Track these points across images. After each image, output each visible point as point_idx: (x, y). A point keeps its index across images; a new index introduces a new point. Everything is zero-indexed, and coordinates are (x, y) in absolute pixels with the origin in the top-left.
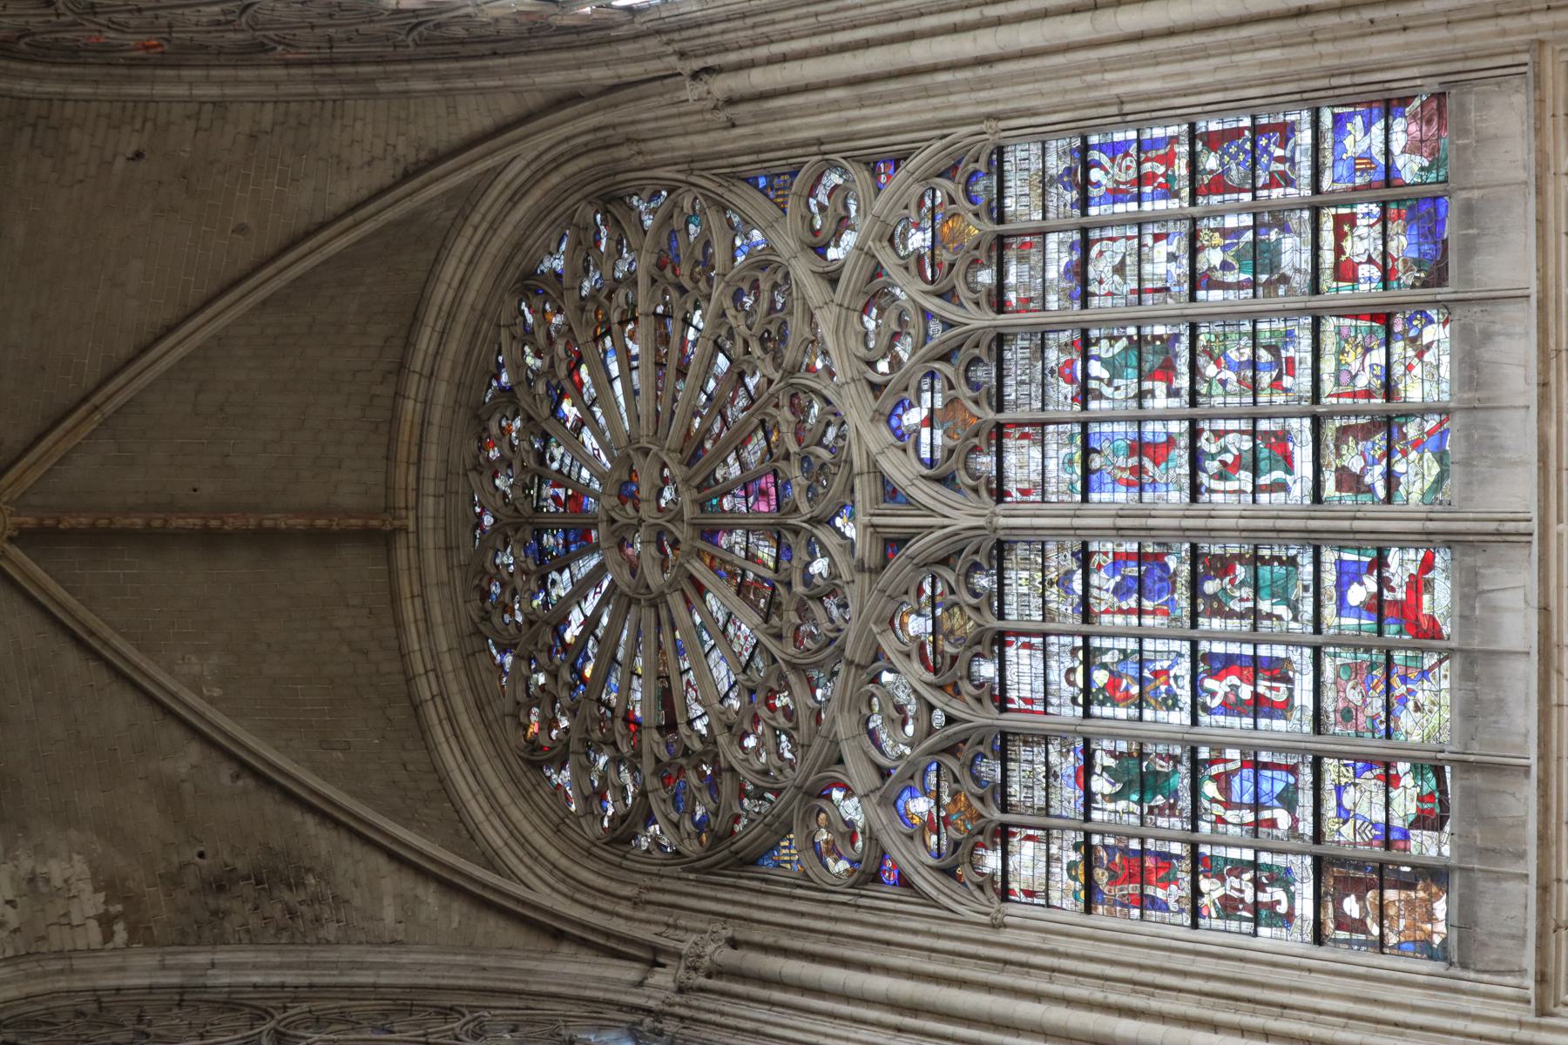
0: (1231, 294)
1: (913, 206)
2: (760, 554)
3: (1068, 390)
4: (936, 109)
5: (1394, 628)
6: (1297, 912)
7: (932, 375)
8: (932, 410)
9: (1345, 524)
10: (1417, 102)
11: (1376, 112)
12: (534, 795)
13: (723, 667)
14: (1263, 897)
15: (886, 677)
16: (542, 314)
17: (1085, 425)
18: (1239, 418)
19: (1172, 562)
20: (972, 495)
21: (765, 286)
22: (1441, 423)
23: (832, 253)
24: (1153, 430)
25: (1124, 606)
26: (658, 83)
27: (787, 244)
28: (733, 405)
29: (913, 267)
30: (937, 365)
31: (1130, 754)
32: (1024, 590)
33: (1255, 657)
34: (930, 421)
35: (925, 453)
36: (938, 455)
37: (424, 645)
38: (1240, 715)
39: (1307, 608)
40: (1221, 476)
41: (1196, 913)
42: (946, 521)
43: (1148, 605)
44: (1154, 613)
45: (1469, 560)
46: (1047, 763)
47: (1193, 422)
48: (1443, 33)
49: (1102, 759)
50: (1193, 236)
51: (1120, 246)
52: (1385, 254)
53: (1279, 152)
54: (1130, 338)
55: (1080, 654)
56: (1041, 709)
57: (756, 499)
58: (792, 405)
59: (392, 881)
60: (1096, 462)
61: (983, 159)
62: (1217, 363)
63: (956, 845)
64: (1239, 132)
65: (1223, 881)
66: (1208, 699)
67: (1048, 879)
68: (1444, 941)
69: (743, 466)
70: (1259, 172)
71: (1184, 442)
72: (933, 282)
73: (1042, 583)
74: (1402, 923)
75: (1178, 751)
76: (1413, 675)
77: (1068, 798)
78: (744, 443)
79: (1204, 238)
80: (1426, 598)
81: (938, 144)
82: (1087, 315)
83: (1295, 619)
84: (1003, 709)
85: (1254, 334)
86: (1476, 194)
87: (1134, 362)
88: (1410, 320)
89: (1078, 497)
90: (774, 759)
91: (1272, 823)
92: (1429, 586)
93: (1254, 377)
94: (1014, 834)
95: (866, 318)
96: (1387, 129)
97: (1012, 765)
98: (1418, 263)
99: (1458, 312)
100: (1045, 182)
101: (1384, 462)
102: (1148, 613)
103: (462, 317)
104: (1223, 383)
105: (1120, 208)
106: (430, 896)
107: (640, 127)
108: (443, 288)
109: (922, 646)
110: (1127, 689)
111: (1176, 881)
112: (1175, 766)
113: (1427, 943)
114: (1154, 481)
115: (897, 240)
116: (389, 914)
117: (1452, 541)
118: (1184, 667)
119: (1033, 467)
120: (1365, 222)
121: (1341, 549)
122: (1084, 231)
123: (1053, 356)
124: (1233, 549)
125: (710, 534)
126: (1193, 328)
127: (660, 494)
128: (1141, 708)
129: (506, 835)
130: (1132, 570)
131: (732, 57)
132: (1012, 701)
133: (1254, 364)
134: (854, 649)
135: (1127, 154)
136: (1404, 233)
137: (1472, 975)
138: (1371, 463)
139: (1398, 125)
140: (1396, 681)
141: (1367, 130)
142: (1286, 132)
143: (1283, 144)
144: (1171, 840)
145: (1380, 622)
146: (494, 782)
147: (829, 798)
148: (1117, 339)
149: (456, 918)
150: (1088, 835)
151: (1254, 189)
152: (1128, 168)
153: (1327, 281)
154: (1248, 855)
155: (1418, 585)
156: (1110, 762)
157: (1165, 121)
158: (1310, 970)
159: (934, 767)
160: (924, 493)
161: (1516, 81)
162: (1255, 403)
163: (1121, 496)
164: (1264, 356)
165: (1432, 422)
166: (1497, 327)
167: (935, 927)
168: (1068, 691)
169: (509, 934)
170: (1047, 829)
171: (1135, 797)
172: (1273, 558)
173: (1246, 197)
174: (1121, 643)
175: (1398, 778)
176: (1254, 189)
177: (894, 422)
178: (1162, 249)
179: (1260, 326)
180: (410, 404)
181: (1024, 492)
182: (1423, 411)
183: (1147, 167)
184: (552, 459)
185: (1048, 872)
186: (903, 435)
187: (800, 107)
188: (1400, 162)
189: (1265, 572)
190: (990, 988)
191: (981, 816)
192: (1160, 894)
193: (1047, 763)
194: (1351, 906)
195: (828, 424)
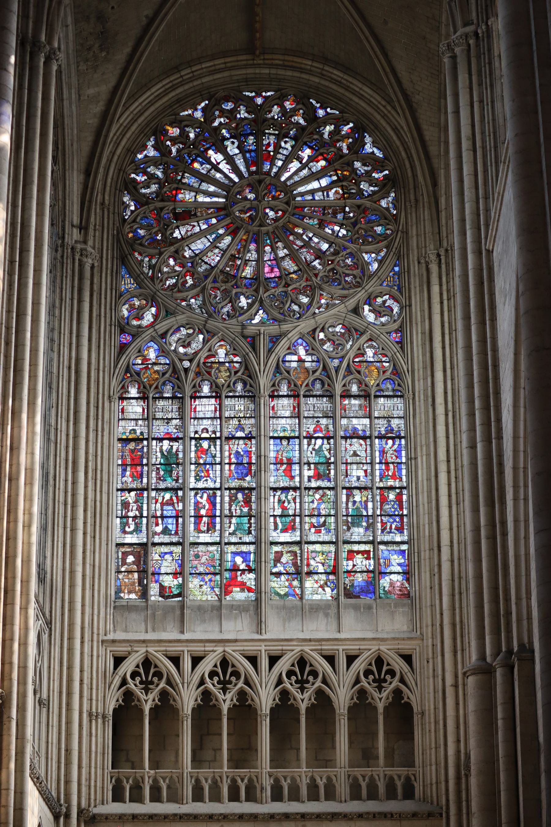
0: (344, 505)
1: (383, 352)
2: (248, 268)
3: (311, 430)
4: (419, 370)
5: (228, 576)
6: (126, 536)
7: (318, 361)
8: (304, 361)
9: (263, 559)
10: (407, 585)
11: (405, 568)
12: (143, 135)
13: (201, 246)
14: (131, 519)
15: (201, 337)
16: (347, 136)
17: (298, 437)
18: (300, 509)
19: (248, 478)
20: (272, 383)
21: (355, 272)
22: (298, 595)
23: (366, 308)
24: (296, 467)
25: (232, 456)
26: (437, 231)
27: (371, 286)
28: (308, 252)
29: (359, 352)
30: (322, 362)
31: (177, 459)
32: (237, 409)
33: (215, 516)
34: (300, 360)
35: (288, 358)
36: (287, 364)
37: (204, 70)
38: (195, 509)
39: (233, 539)
40: (279, 500)
41: (122, 490)
42: (262, 373)
43: (233, 467)
44: (230, 470)
45: (252, 608)
46: (172, 419)
47: (299, 488)
48: (429, 604)
49: (175, 445)
50: (365, 488)
51: (363, 454)
52: (356, 572)
53: (393, 527)
54: (330, 459)
55: (213, 436)
56: (192, 416)
57: (269, 266)
58: (307, 286)
59: (105, 89)
60: (285, 442)
61: (399, 388)
62: (320, 499)
63: (138, 374)
64: (401, 508)
65: (135, 502)
66: (199, 495)
67: (129, 419)
68: (122, 598)
69: (283, 258)
70: (387, 518)
71: (292, 484)
72: (353, 362)
73: (239, 417)
74: (127, 580)
75: (180, 481)
76: (212, 584)
77: (160, 429)
78: (292, 259)
79: (365, 493)
80: (238, 589)
81: (406, 369)
82: (338, 438)
83: (230, 534)
84: (191, 397)
85: (330, 515)
86: (375, 611)
87: (321, 461)
88: (333, 582)
89: (271, 435)
90: (166, 276)
91: (157, 525)
92: (242, 590)
93: (314, 515)
94: (144, 403)
95: (341, 326)
96: (399, 573)
97: (170, 401)
98: (352, 586)
99: (335, 603)
100: (389, 418)
101: (285, 572)
102: (230, 467)
103: (347, 94)
104: (313, 502)
105: (377, 454)
106: (98, 108)
107: (422, 209)
108: (360, 85)
109: (214, 356)
110: (201, 457)
111: (133, 481)
112: (174, 480)
113: (121, 592)
114: (278, 470)
115: (370, 343)
116: (91, 91)
117: (258, 601)
118: (211, 485)
119: (283, 412)
120: (367, 564)
121: (255, 553)
122: (370, 437)
123: (324, 421)
124: (254, 506)
125: (257, 239)
126: (332, 489)
127: (272, 209)
128: (195, 464)
129: (125, 124)
130: (245, 460)
131: (444, 279)
132: (194, 402)
133: (319, 515)
134: (211, 324)
135: (397, 457)
136: (363, 580)
137: (112, 612)
138: (284, 564)
139: (400, 577)
140: (210, 576)
141: (399, 565)
142: (400, 530)
143: (397, 529)
144: (148, 478)
145: (229, 570)
146: (146, 114)
147: (152, 306)
148: (330, 453)
149: (91, 122)
150: (147, 439)
151: (381, 515)
152: (392, 458)
153: (347, 547)
154: (145, 514)
155: (243, 586)
156: (174, 450)
157: (407, 476)
158: (107, 544)
159: (168, 362)
161: (411, 627)
162: (306, 516)
163: (272, 454)
164: (322, 520)
165: (298, 591)
166: (330, 619)
167: (107, 369)
168: (199, 429)
169: (86, 148)
170: (148, 419)
171: (162, 461)
172: (250, 524)
173: (378, 512)
174: (218, 455)
175: (176, 578)
176: (381, 515)
177: (300, 341)
178: (361, 473)
179: (333, 517)
180: (310, 63)
181: (273, 408)
182: (302, 587)
183: (391, 466)
184: (286, 142)
185: (132, 419)
186: (295, 346)
187: (423, 296)
188: (387, 578)
189: (246, 520)
190: (88, 403)
191: (150, 387)
192: (128, 473)
193: (172, 419)
194: (130, 559)
195: (300, 307)
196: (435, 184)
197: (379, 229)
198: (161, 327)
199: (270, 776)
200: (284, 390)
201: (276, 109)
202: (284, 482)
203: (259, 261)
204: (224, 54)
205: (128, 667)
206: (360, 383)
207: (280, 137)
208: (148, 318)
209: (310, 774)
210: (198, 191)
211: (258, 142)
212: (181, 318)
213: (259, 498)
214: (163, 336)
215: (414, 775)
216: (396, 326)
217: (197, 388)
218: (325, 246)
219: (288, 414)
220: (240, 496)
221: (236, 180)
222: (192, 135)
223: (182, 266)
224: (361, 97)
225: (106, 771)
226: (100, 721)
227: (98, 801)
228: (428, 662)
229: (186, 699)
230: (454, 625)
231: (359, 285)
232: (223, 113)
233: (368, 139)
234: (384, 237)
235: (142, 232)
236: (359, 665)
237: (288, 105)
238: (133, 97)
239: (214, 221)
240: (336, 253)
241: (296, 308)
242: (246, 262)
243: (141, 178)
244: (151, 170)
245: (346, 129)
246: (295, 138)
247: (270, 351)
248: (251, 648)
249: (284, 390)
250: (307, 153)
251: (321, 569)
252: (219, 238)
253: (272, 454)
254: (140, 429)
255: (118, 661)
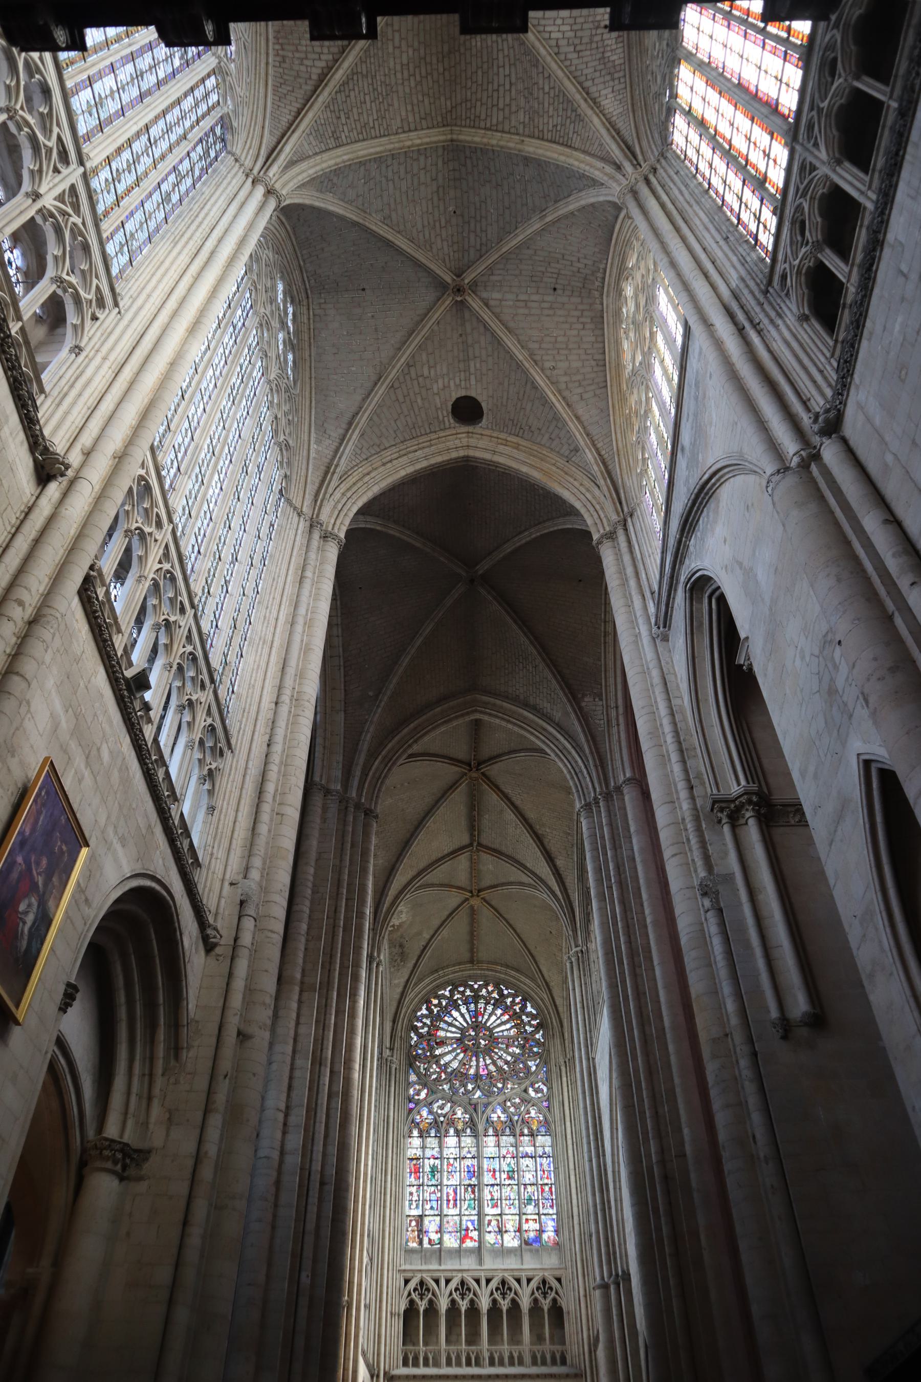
15: (449, 1105)
16: (518, 1003)
19: (473, 1179)
24: (497, 1174)
27: (532, 1078)
34: (499, 1117)
39: (466, 1213)
77: (428, 1153)
106: (400, 990)
116: (396, 982)
123: (511, 1149)
142: (552, 1207)
153: (524, 1217)
160: (485, 1116)
194: (414, 1223)
196: (562, 1026)
197: (535, 1050)
198: (430, 1100)
200: (491, 1132)
201: (484, 990)
202: (492, 1182)
203: (478, 1066)
204: (460, 964)
205: (412, 1285)
206: (529, 1128)
207: (487, 1003)
208: (423, 1095)
210: (447, 1031)
211: (476, 1006)
212: (439, 1095)
213: (479, 1190)
214: (431, 1104)
216: (545, 1098)
217: (447, 1131)
218: (509, 1058)
219: (493, 1144)
220: (469, 1189)
221: (465, 1025)
222: (444, 1003)
223: (440, 1068)
224: (525, 984)
230: (582, 1261)
231: (527, 1077)
232: (459, 992)
233: (529, 1005)
234: (538, 1053)
235: (420, 1052)
236: (534, 1284)
237: (490, 988)
238: (416, 985)
239: (455, 1046)
240: (515, 1062)
241: (495, 1089)
242: (471, 1067)
243: (419, 1024)
244: (424, 1020)
245: (518, 1000)
246: (494, 1005)
247: (483, 1112)
248: (476, 1274)
249: (491, 1132)
250: (499, 1012)
251: (512, 1229)
252: (458, 1054)
253: (485, 1167)
254: (419, 1153)
255: (407, 1282)
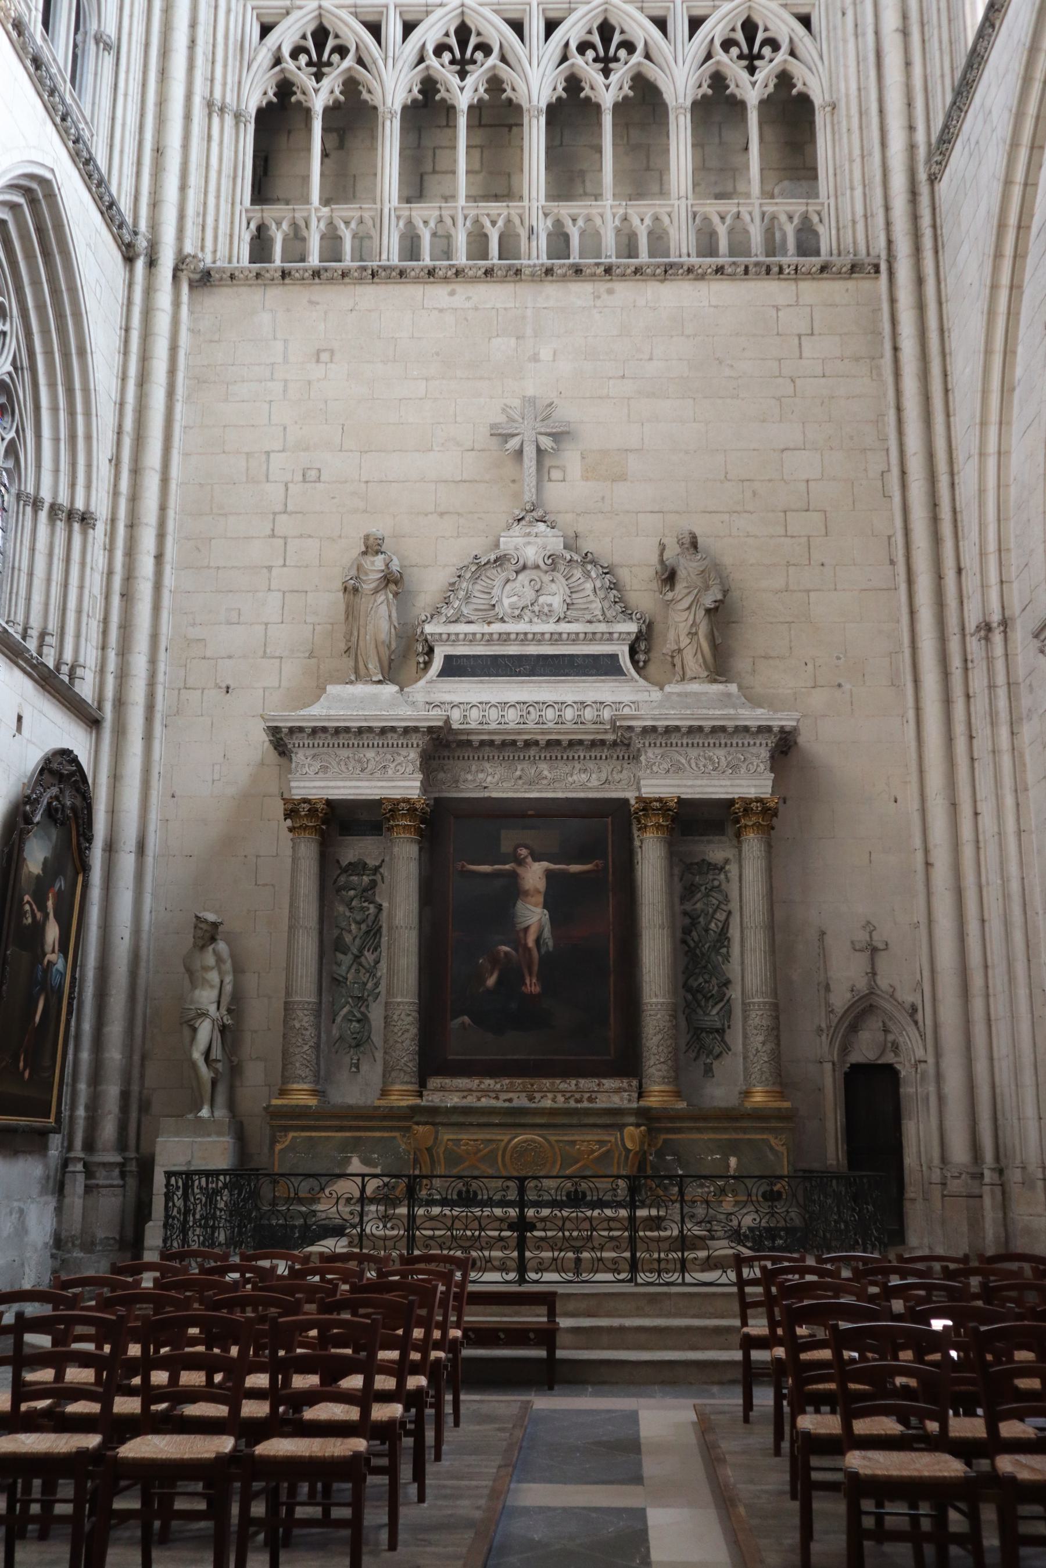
199: (546, 215)
205: (286, 36)
209: (621, 211)
215: (819, 214)
225: (238, 207)
226: (229, 120)
227: (219, 254)
228: (844, 14)
229: (389, 85)
